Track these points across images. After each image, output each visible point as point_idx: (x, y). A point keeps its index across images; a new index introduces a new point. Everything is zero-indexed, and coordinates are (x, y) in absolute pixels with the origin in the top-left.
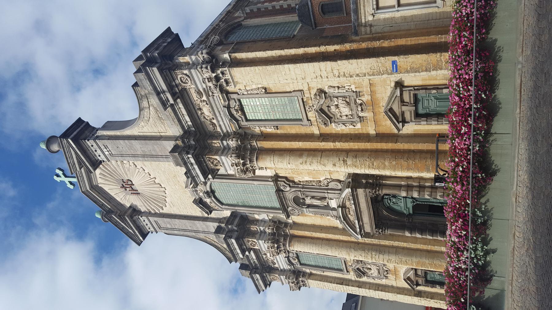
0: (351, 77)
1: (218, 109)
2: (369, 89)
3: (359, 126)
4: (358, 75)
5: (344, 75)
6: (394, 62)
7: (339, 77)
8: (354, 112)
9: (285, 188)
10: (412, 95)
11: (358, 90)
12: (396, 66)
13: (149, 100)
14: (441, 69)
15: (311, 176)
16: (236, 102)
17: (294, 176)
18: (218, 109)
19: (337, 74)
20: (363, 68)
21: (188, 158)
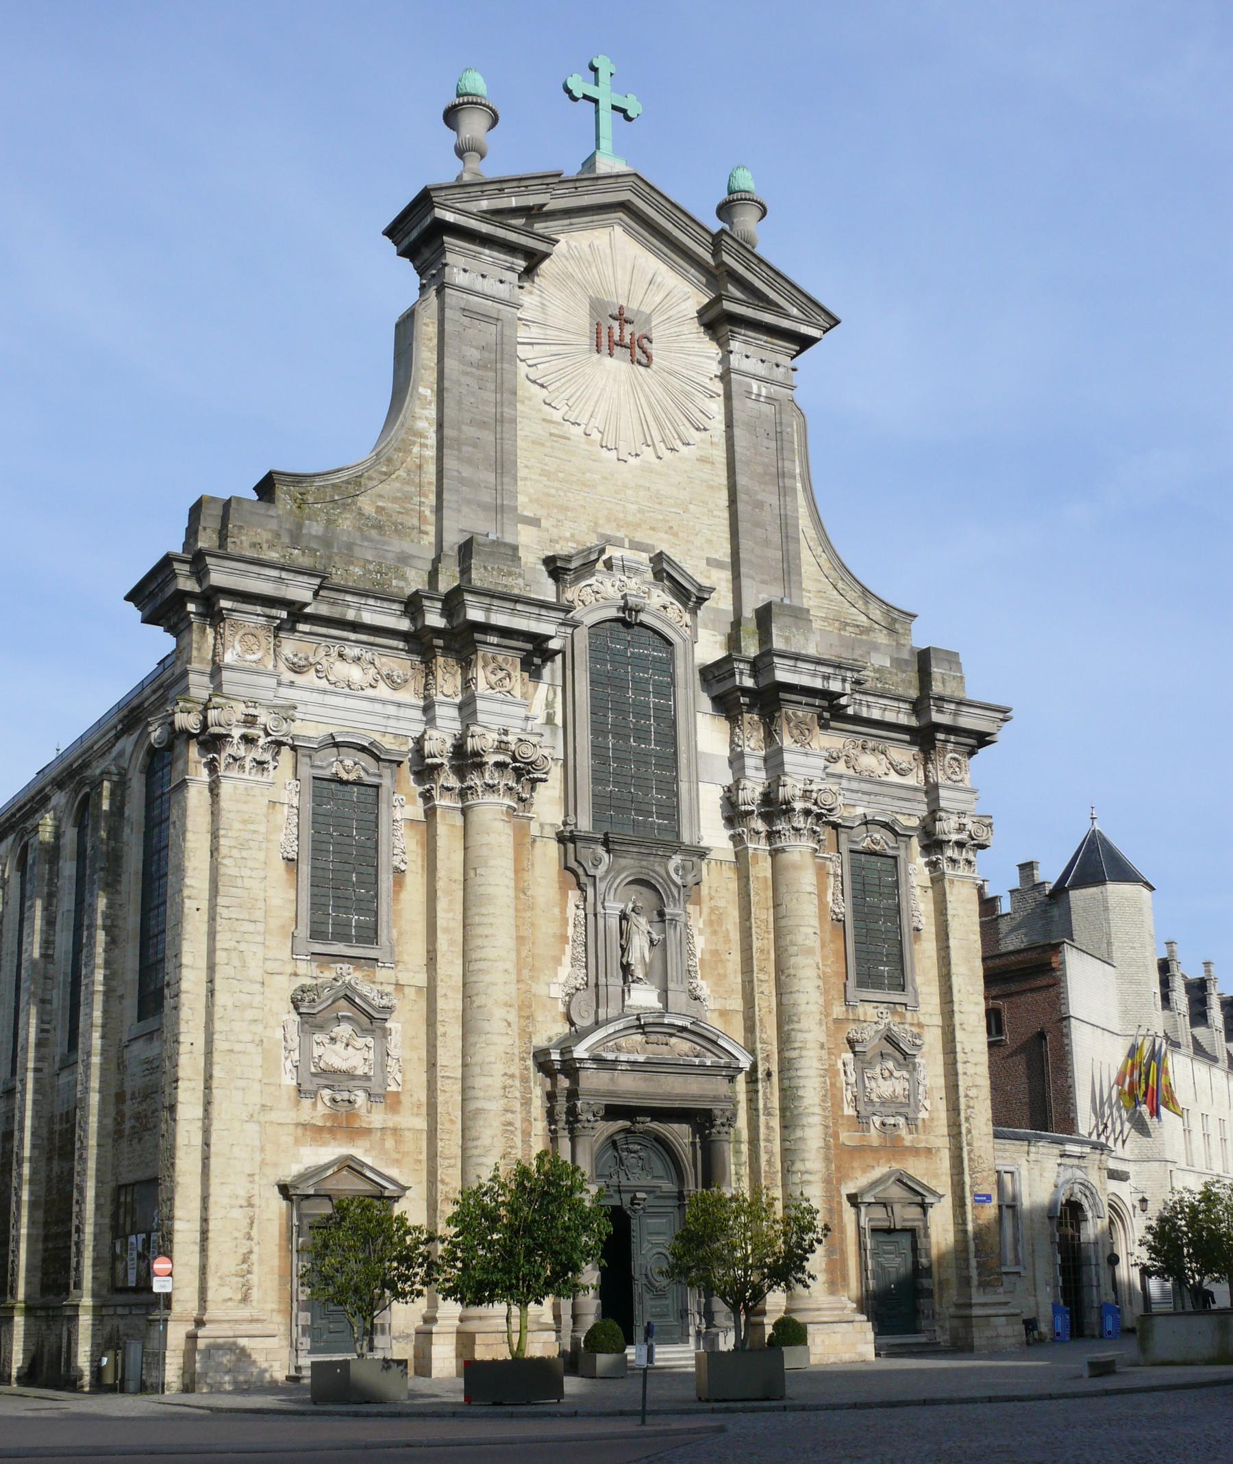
0: (967, 1119)
1: (876, 794)
2: (923, 1145)
3: (849, 1111)
4: (969, 1131)
5: (969, 1107)
6: (989, 1197)
7: (967, 1096)
8: (877, 1108)
9: (676, 871)
10: (916, 1223)
11: (920, 1123)
12: (984, 1201)
13: (885, 632)
14: (979, 1275)
15: (707, 957)
16: (893, 848)
17: (706, 911)
18: (876, 794)
19: (971, 1093)
20: (980, 1144)
21: (844, 680)
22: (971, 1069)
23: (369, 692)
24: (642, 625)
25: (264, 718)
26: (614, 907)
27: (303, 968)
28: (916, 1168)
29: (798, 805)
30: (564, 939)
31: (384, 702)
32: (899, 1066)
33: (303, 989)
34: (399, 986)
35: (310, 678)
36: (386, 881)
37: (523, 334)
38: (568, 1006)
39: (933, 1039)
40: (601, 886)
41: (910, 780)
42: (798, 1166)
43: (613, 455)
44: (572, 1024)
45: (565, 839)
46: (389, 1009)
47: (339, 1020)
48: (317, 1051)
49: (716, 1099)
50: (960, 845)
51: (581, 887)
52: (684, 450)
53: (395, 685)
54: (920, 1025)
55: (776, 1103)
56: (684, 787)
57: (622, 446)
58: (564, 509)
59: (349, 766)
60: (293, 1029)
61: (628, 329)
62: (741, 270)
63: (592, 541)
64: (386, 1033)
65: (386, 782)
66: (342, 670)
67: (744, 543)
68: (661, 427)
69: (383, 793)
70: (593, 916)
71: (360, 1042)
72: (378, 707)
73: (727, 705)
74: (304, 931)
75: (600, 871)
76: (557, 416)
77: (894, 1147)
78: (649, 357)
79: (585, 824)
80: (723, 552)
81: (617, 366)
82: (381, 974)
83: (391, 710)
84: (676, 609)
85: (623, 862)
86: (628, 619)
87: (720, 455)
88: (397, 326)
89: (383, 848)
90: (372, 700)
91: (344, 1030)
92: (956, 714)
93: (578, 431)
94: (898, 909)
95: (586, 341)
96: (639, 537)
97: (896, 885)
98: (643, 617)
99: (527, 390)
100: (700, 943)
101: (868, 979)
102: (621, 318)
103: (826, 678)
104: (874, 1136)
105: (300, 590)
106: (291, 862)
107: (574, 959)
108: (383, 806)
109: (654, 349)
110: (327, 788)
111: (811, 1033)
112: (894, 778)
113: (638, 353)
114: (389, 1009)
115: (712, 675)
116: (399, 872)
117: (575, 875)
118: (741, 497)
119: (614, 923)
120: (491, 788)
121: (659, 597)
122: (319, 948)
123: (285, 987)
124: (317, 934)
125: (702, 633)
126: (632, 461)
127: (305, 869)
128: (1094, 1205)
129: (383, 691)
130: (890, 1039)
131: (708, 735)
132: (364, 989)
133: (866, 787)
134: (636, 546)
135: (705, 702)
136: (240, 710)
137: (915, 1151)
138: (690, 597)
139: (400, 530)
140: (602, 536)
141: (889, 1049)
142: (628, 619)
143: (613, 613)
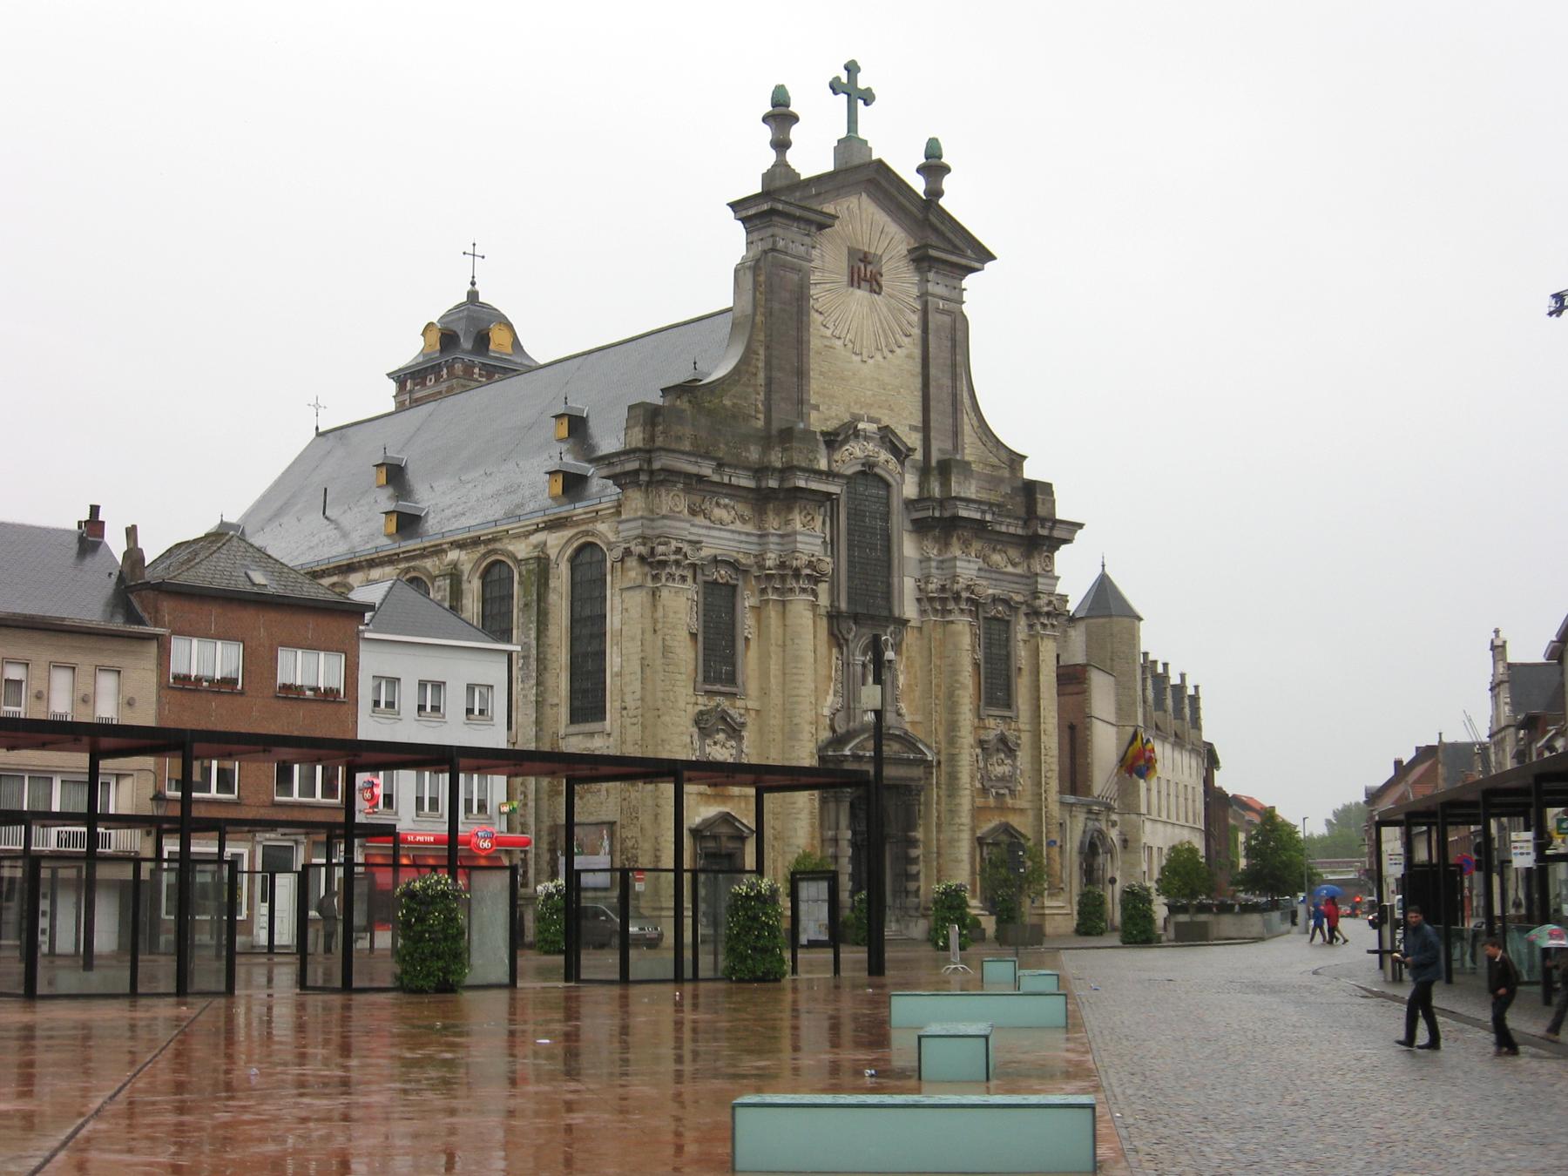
22: (1049, 760)
23: (731, 527)
24: (876, 475)
25: (686, 548)
26: (859, 658)
27: (700, 700)
28: (1015, 821)
29: (965, 595)
30: (830, 677)
31: (740, 533)
32: (1008, 757)
33: (701, 713)
34: (747, 709)
35: (700, 520)
36: (740, 644)
37: (814, 278)
38: (832, 720)
39: (1025, 739)
40: (852, 645)
41: (1019, 571)
42: (957, 820)
43: (858, 358)
44: (834, 731)
45: (834, 616)
46: (743, 725)
47: (718, 731)
48: (708, 750)
49: (912, 779)
50: (1048, 614)
51: (840, 647)
52: (898, 351)
53: (744, 521)
54: (1019, 730)
55: (943, 780)
56: (896, 580)
57: (865, 352)
58: (832, 397)
59: (722, 575)
60: (696, 737)
61: (869, 268)
62: (938, 224)
63: (847, 418)
64: (741, 738)
65: (740, 583)
66: (719, 513)
67: (933, 416)
68: (886, 336)
69: (739, 590)
70: (847, 664)
71: (728, 744)
72: (736, 536)
73: (921, 528)
74: (700, 678)
75: (851, 637)
76: (828, 333)
77: (1002, 808)
78: (881, 287)
79: (843, 606)
80: (917, 420)
81: (861, 294)
82: (739, 703)
83: (743, 538)
84: (893, 463)
85: (864, 630)
86: (868, 472)
87: (917, 352)
88: (736, 271)
89: (739, 625)
90: (733, 532)
91: (721, 736)
92: (1051, 529)
93: (839, 343)
94: (1008, 656)
95: (845, 279)
96: (874, 413)
97: (1008, 640)
98: (877, 470)
99: (815, 316)
100: (901, 679)
101: (991, 702)
102: (865, 258)
103: (984, 512)
104: (992, 801)
105: (707, 469)
106: (694, 636)
107: (836, 692)
108: (739, 599)
109: (884, 281)
110: (711, 587)
111: (967, 737)
112: (1010, 569)
113: (875, 287)
114: (743, 725)
115: (909, 504)
116: (747, 639)
117: (837, 639)
118: (932, 384)
119: (859, 669)
120: (804, 590)
121: (884, 455)
122: (708, 687)
123: (692, 711)
124: (706, 680)
125: (907, 476)
126: (871, 361)
127: (700, 638)
128: (1103, 844)
129: (738, 526)
130: (1003, 739)
131: (908, 548)
132: (731, 712)
133: (994, 576)
134: (871, 420)
135: (908, 526)
136: (674, 544)
137: (1014, 810)
138: (900, 453)
139: (747, 418)
140: (853, 415)
141: (1001, 746)
142: (868, 472)
143: (859, 468)
